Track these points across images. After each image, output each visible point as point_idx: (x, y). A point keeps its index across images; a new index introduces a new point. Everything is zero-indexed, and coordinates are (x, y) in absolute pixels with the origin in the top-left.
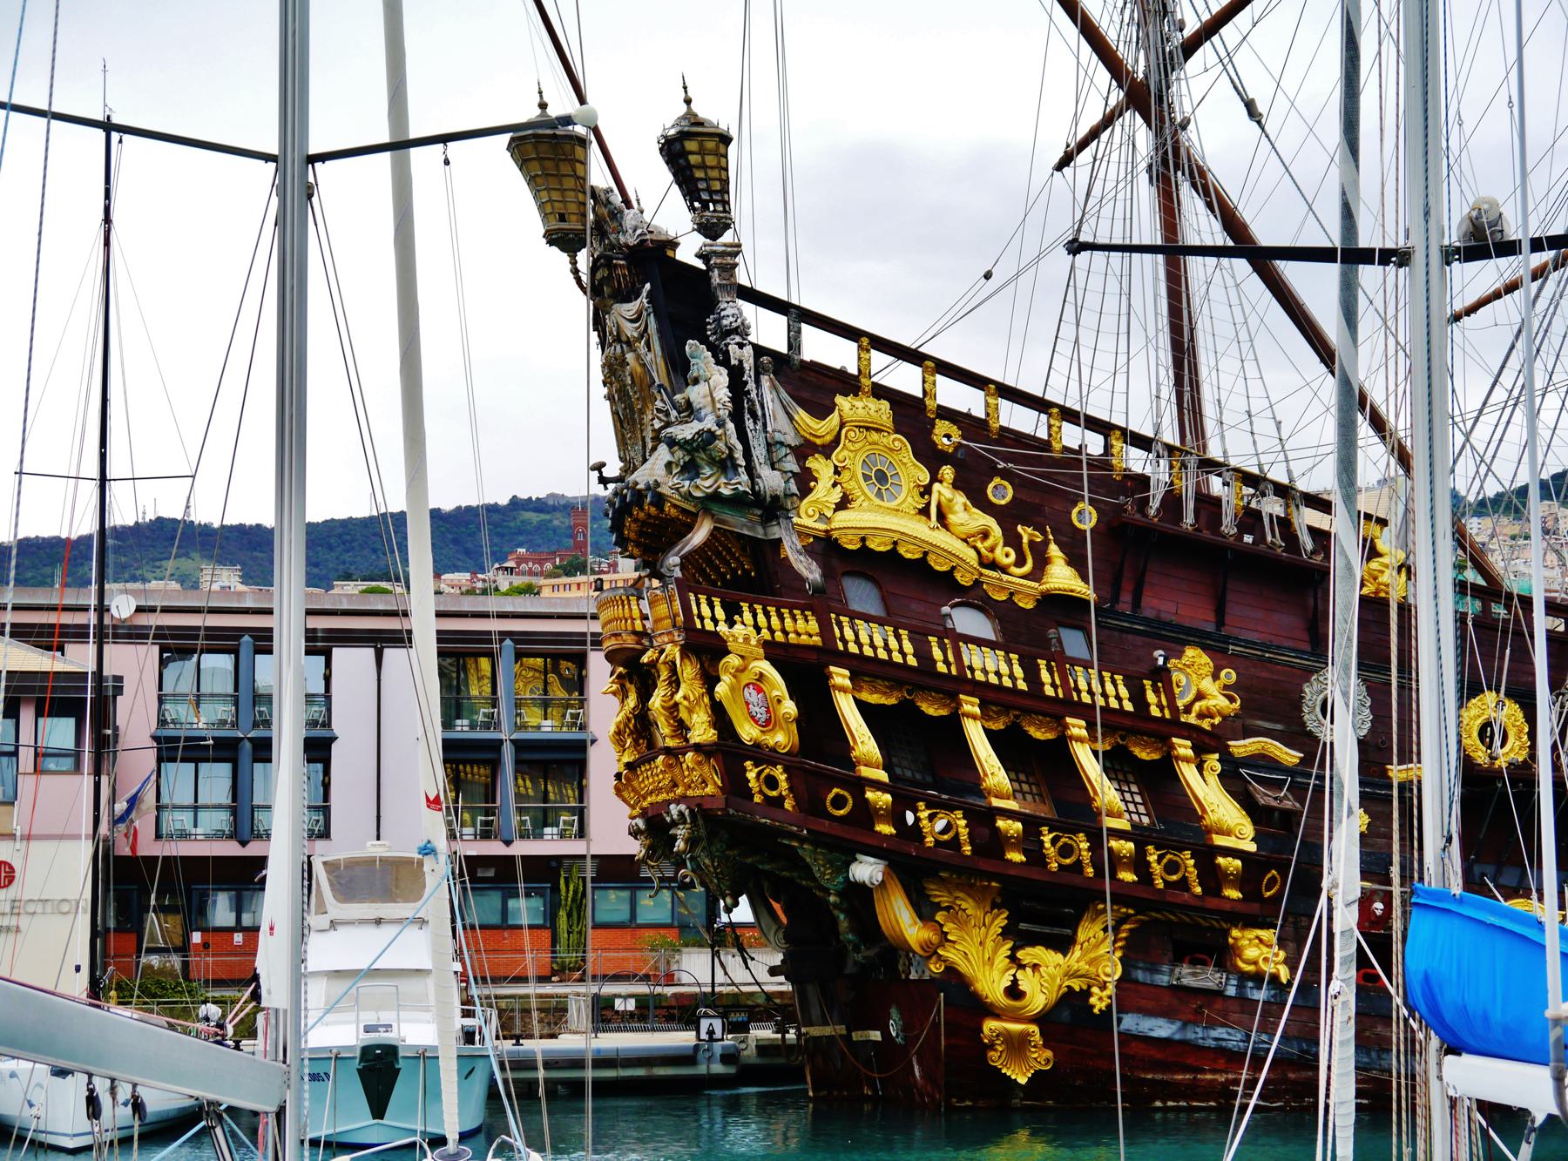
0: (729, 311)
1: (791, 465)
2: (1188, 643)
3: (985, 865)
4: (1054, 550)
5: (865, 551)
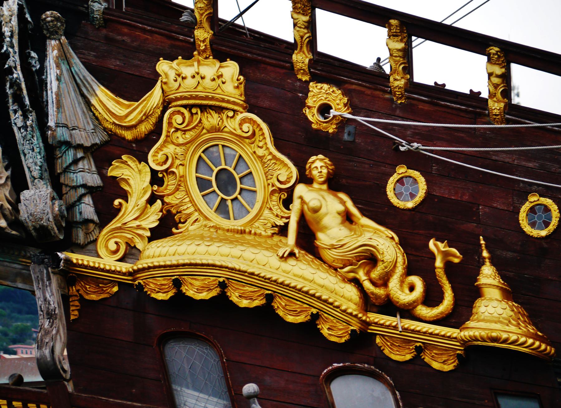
1: (86, 175)
4: (488, 275)
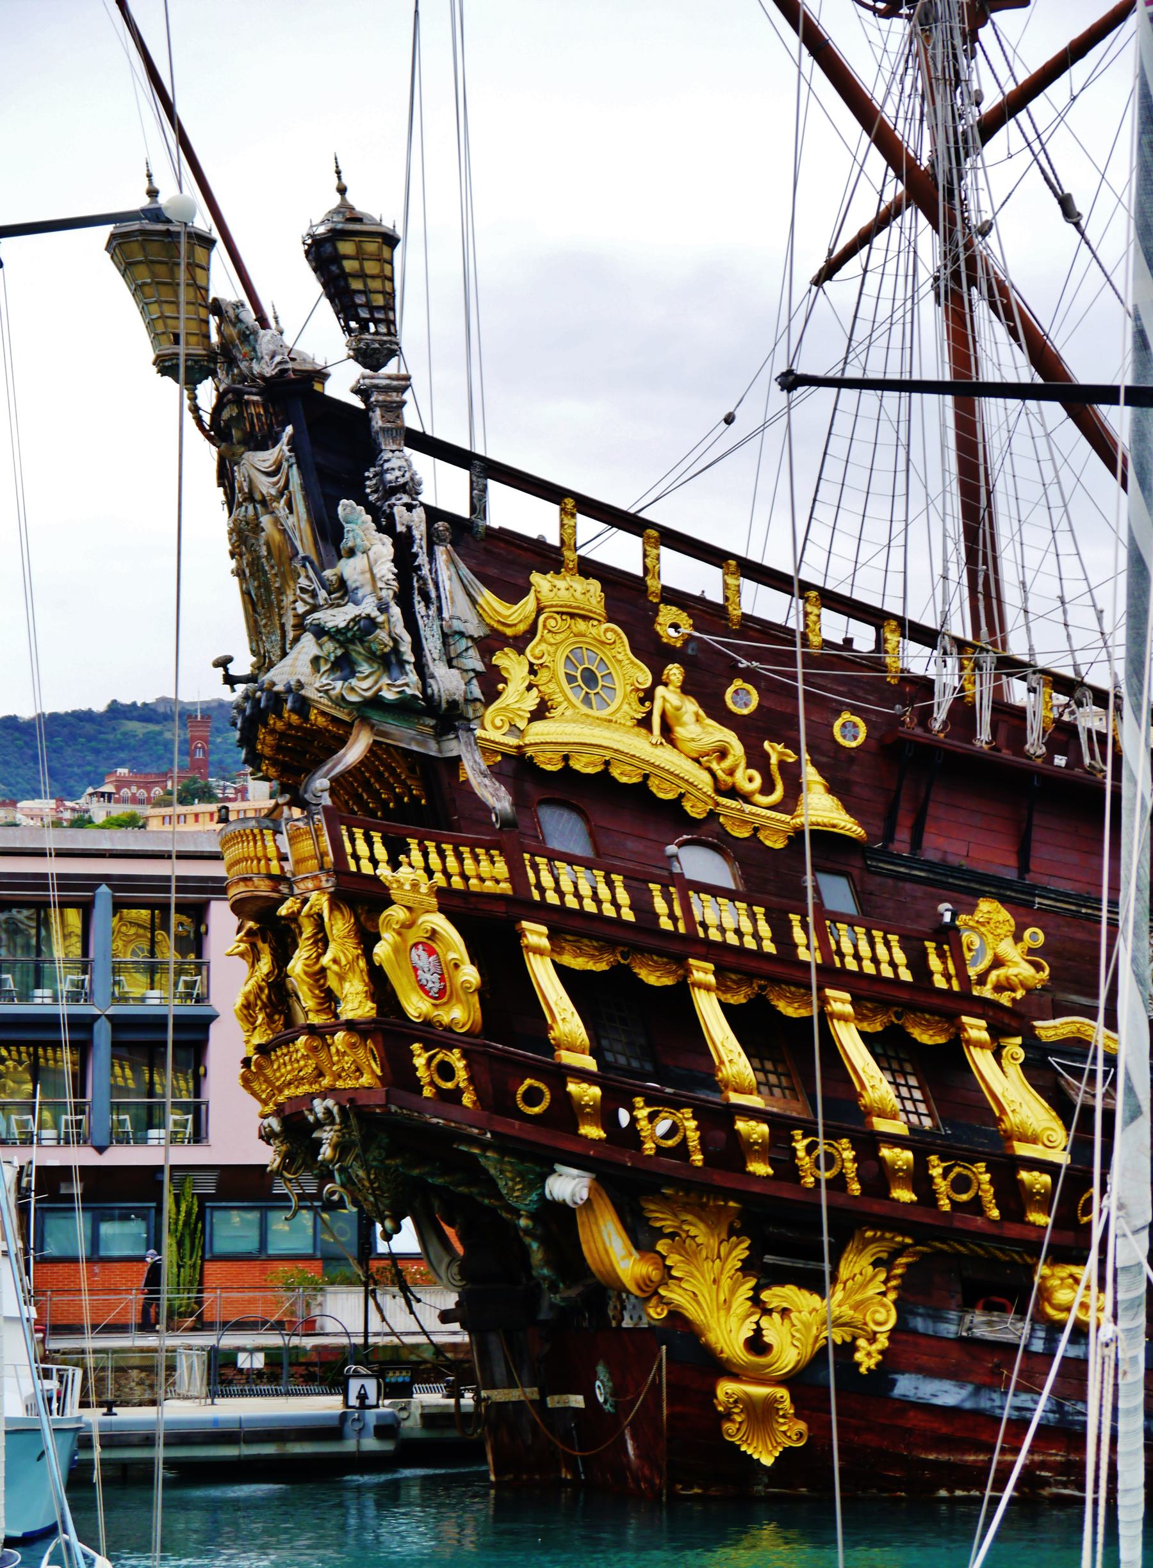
0: (394, 463)
1: (473, 661)
2: (984, 894)
3: (719, 1178)
4: (810, 774)
5: (567, 771)
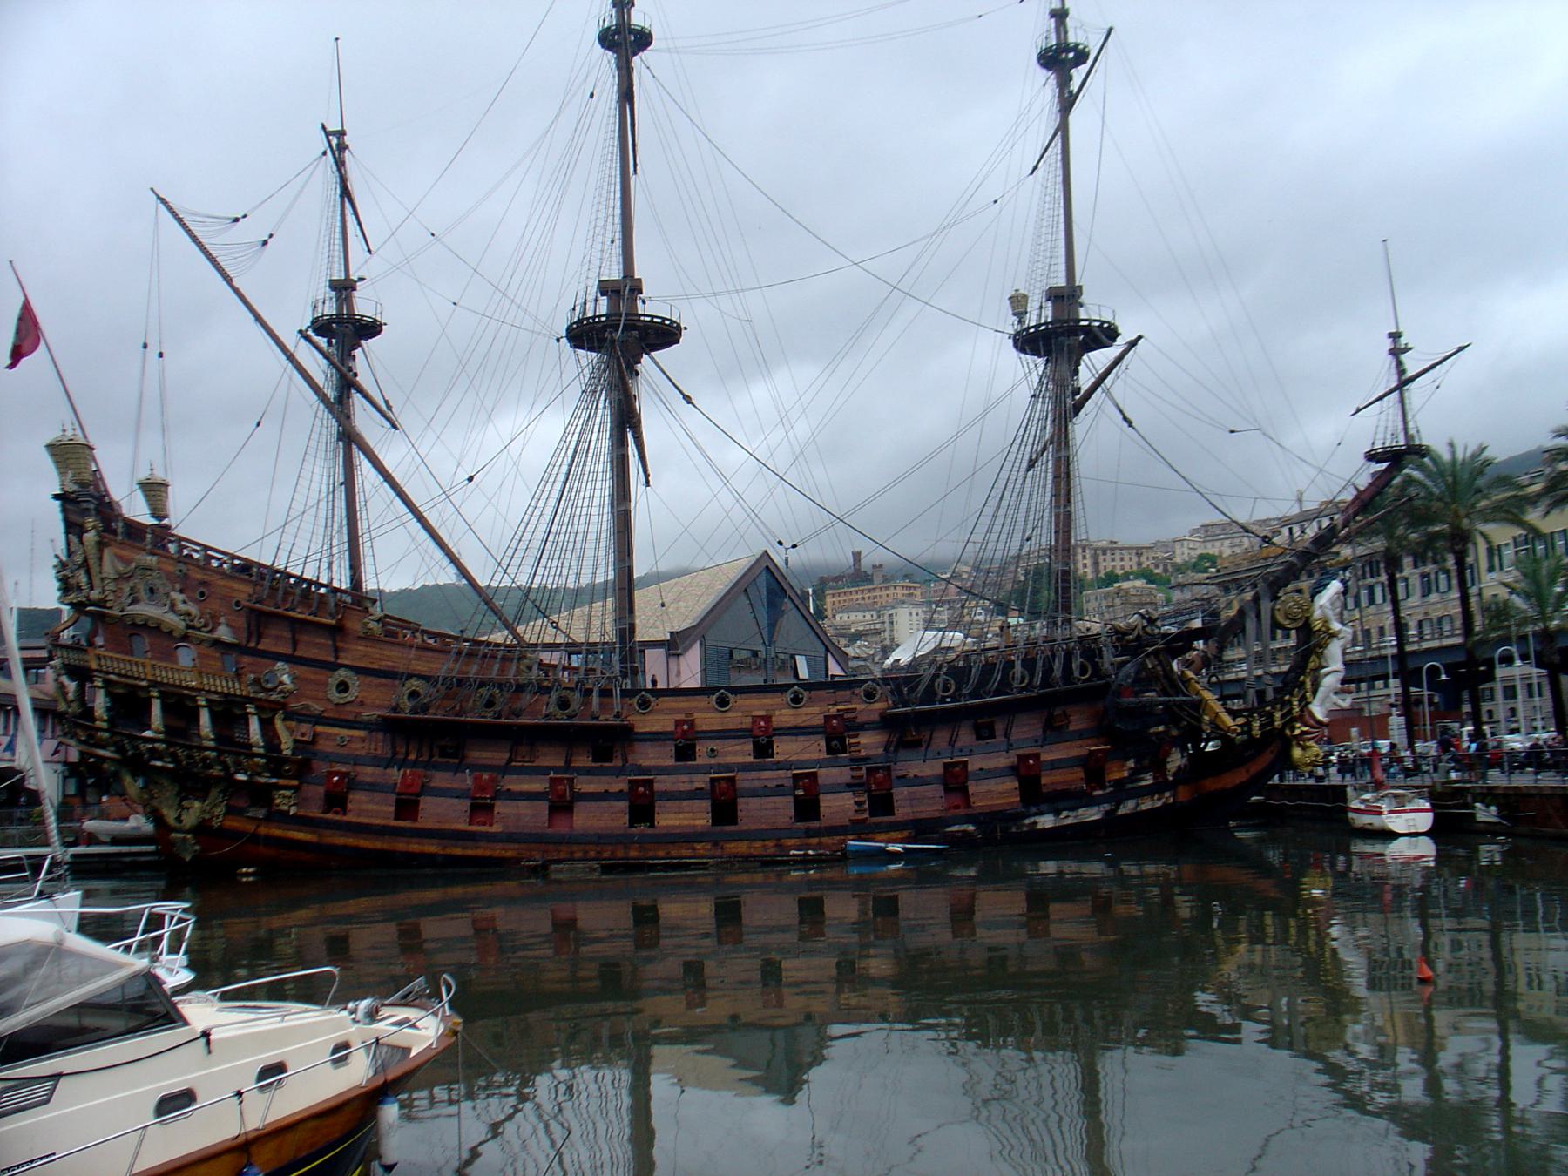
1: (111, 586)
